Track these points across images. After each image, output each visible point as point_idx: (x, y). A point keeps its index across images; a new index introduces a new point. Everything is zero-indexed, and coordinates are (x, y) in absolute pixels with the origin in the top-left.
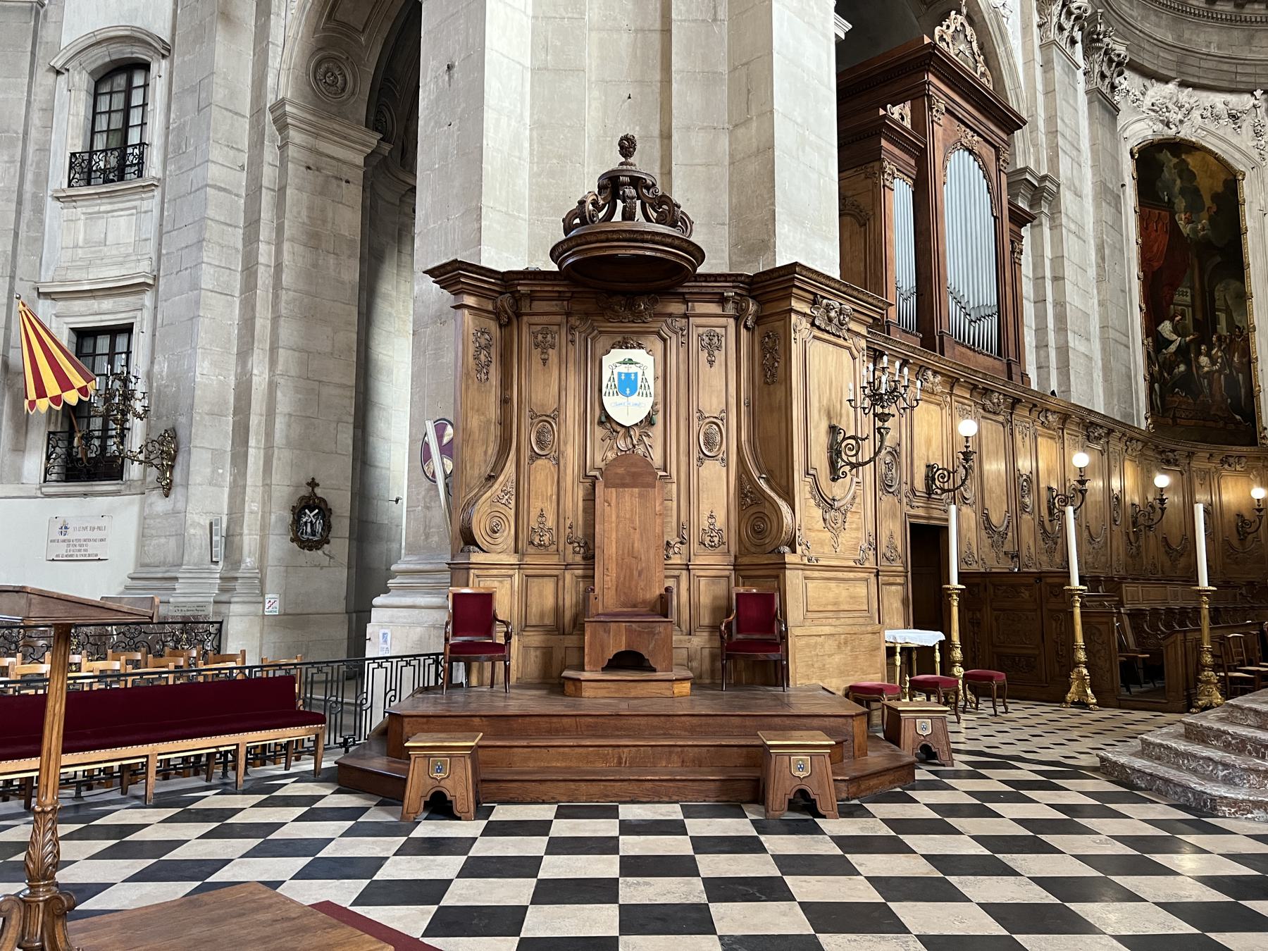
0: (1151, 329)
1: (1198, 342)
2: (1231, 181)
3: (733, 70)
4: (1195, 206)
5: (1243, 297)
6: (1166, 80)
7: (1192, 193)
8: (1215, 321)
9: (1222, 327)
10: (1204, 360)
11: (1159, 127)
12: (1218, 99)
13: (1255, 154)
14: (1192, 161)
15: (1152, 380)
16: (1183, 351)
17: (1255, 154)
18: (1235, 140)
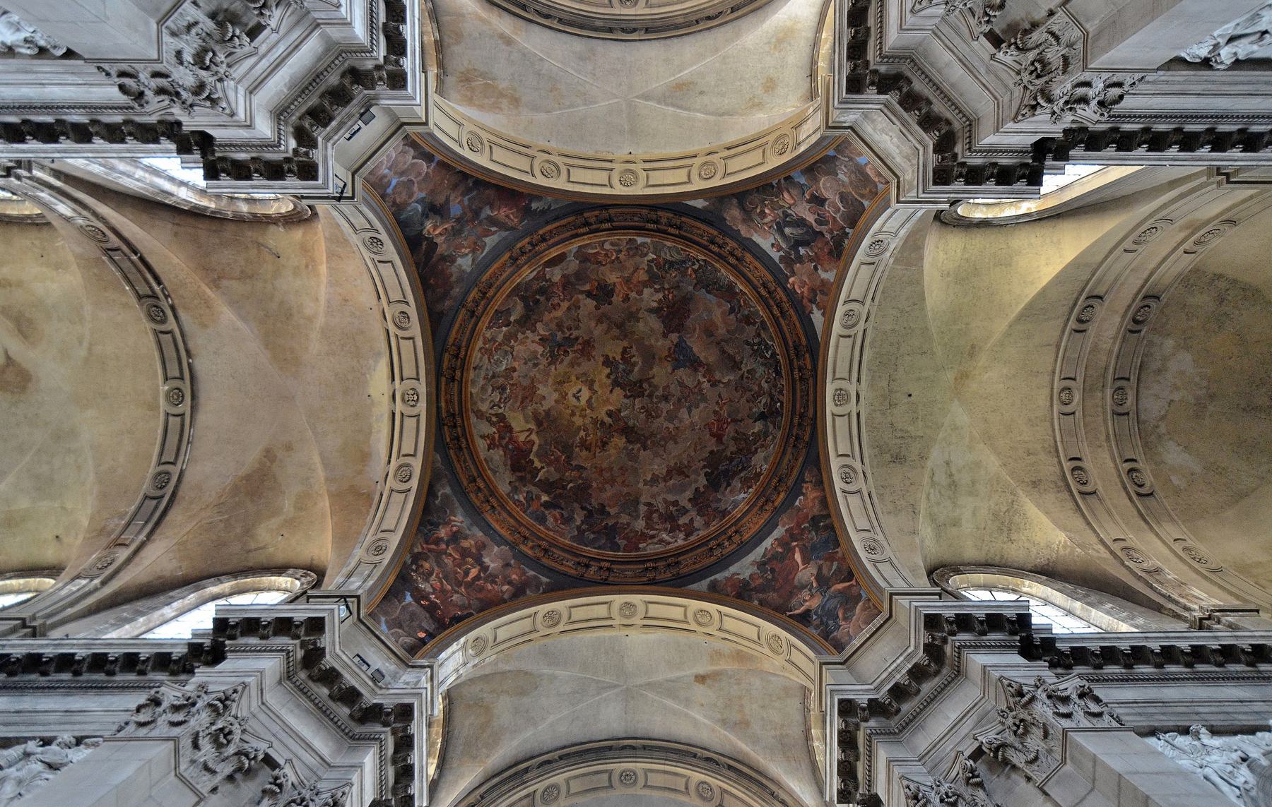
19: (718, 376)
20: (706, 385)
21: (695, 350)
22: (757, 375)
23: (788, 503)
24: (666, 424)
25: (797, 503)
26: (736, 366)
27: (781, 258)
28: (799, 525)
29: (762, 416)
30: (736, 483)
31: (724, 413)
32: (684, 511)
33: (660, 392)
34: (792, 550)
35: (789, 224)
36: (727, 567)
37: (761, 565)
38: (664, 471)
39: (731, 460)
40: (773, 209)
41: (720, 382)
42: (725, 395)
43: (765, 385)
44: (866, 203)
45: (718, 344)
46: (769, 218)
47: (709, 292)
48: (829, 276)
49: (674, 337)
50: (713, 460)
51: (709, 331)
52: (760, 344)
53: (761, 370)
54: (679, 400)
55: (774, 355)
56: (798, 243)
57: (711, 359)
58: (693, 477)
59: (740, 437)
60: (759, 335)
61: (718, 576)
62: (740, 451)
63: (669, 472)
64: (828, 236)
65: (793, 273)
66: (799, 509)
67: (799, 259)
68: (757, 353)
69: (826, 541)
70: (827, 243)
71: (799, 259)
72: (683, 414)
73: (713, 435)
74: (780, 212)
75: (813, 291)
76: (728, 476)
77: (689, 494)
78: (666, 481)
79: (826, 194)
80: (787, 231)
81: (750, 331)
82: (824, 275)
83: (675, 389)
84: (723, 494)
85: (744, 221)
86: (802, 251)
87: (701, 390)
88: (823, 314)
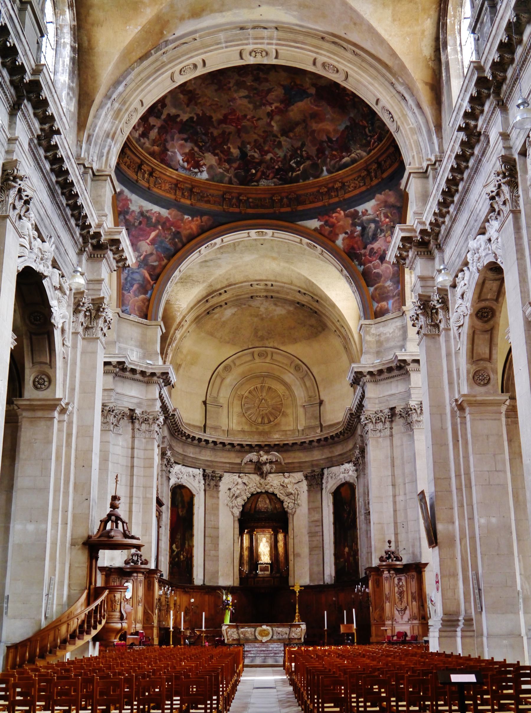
0: (171, 548)
1: (181, 551)
2: (192, 496)
3: (143, 523)
4: (183, 507)
5: (192, 536)
6: (179, 464)
7: (183, 501)
8: (185, 544)
9: (187, 546)
10: (182, 557)
11: (176, 479)
12: (190, 470)
13: (198, 489)
14: (183, 491)
15: (171, 563)
16: (177, 553)
17: (198, 489)
18: (193, 484)
19: (277, 118)
20: (269, 109)
21: (300, 104)
22: (276, 150)
23: (184, 209)
24: (232, 82)
25: (186, 217)
26: (285, 132)
27: (357, 212)
28: (173, 224)
29: (244, 154)
30: (189, 146)
31: (245, 123)
32: (158, 117)
33: (261, 75)
34: (155, 227)
35: (377, 228)
36: (132, 191)
37: (142, 213)
38: (190, 88)
39: (206, 134)
40: (387, 223)
41: (272, 119)
42: (260, 123)
43: (269, 156)
44: (372, 289)
45: (304, 121)
46: (383, 219)
47: (347, 127)
48: (340, 242)
49: (313, 91)
50: (205, 121)
51: (316, 116)
52: (301, 156)
53: (281, 154)
54: (256, 89)
55: (293, 170)
56: (364, 229)
57: (291, 114)
58: (188, 109)
59: (225, 137)
60: (309, 158)
61: (127, 192)
62: (214, 139)
63: (190, 92)
64: (363, 251)
65: (346, 216)
66: (182, 220)
67: (354, 225)
68: (294, 153)
69: (168, 249)
70: (359, 249)
71: (354, 225)
72: (243, 93)
73: (225, 116)
74: (384, 228)
75: (333, 226)
76: (192, 138)
77: (173, 111)
78: (182, 92)
79: (385, 265)
80: (373, 226)
81: (313, 151)
82: (341, 236)
83: (265, 86)
84: (178, 140)
85: (386, 202)
86: (359, 228)
87: (264, 105)
88: (316, 230)
